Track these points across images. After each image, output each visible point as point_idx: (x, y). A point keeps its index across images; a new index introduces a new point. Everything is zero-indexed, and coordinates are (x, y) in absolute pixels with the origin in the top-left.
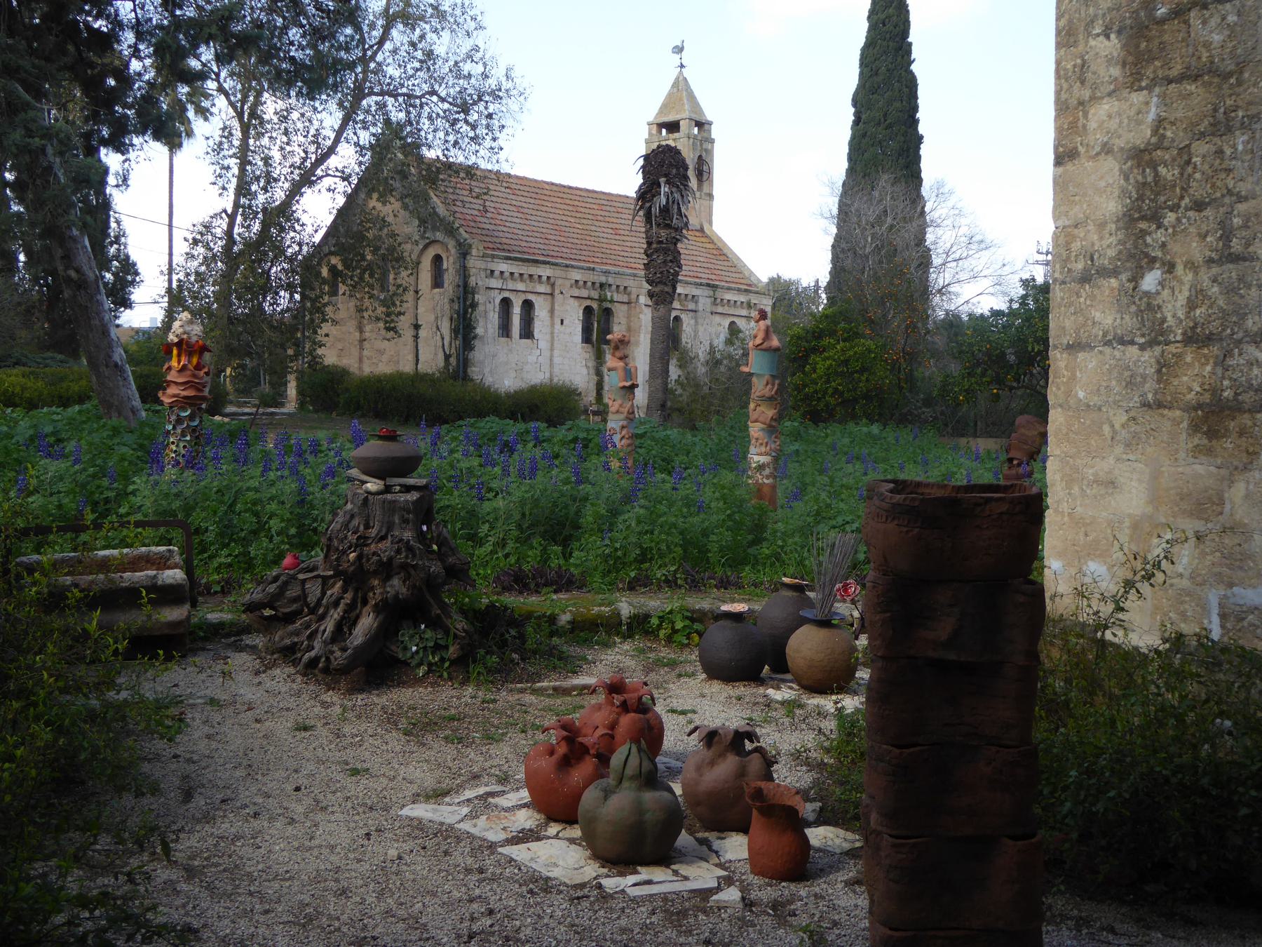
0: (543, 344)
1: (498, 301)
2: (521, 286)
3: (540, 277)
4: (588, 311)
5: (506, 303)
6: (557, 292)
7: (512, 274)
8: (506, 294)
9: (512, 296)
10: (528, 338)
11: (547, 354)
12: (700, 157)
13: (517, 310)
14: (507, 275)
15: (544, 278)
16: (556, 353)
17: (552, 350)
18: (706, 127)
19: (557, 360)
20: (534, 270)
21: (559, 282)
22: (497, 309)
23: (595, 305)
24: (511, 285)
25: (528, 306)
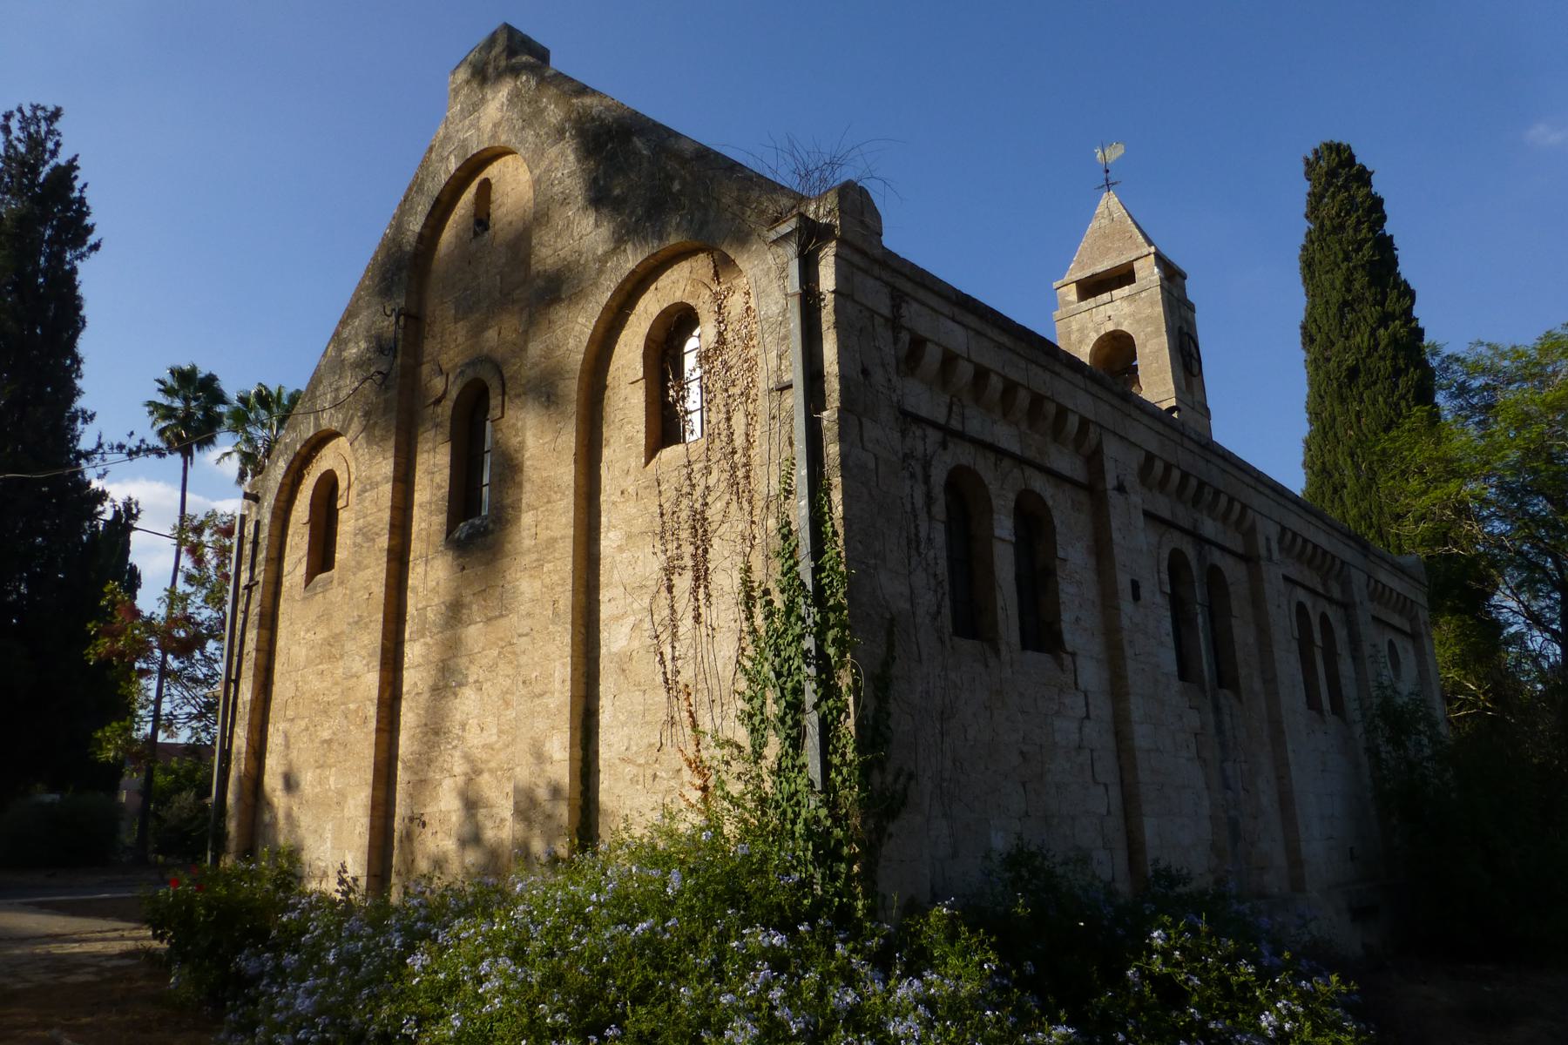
0: (1091, 674)
1: (939, 475)
2: (1005, 436)
3: (1062, 412)
4: (1177, 565)
5: (964, 499)
6: (1111, 482)
7: (981, 374)
8: (962, 455)
9: (984, 467)
10: (1039, 649)
11: (1102, 708)
12: (1180, 328)
13: (1004, 527)
14: (965, 372)
15: (1073, 422)
16: (1137, 708)
17: (1118, 688)
18: (1178, 279)
19: (1142, 736)
20: (1040, 380)
21: (1111, 448)
22: (939, 509)
23: (1190, 552)
24: (976, 425)
25: (1033, 522)
